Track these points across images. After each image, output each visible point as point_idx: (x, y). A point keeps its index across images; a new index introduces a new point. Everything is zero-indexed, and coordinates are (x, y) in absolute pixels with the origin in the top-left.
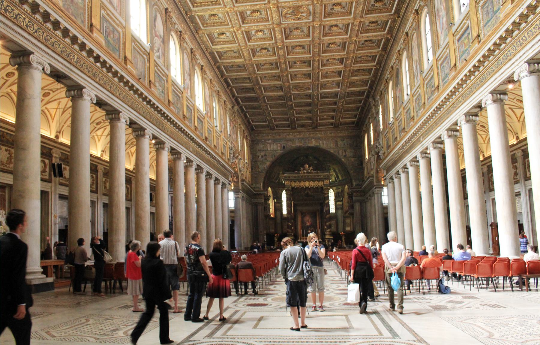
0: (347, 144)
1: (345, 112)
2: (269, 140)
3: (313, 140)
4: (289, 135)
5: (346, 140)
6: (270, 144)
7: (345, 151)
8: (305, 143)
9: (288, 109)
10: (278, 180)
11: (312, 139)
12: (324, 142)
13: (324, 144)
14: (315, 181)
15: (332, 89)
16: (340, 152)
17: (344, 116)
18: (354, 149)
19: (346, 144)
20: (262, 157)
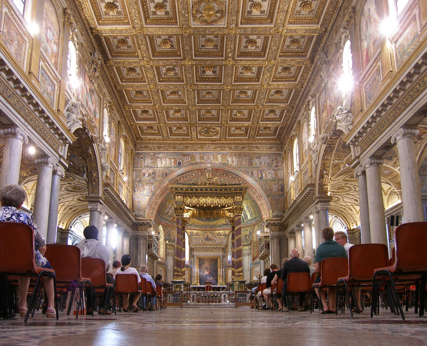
0: (265, 163)
1: (268, 102)
2: (160, 154)
3: (219, 156)
4: (187, 147)
5: (262, 158)
6: (161, 159)
7: (261, 171)
8: (208, 158)
9: (187, 84)
10: (172, 218)
11: (218, 154)
12: (234, 159)
13: (233, 163)
14: (221, 197)
15: (260, 24)
16: (254, 173)
17: (265, 117)
18: (273, 170)
19: (263, 163)
20: (149, 175)
